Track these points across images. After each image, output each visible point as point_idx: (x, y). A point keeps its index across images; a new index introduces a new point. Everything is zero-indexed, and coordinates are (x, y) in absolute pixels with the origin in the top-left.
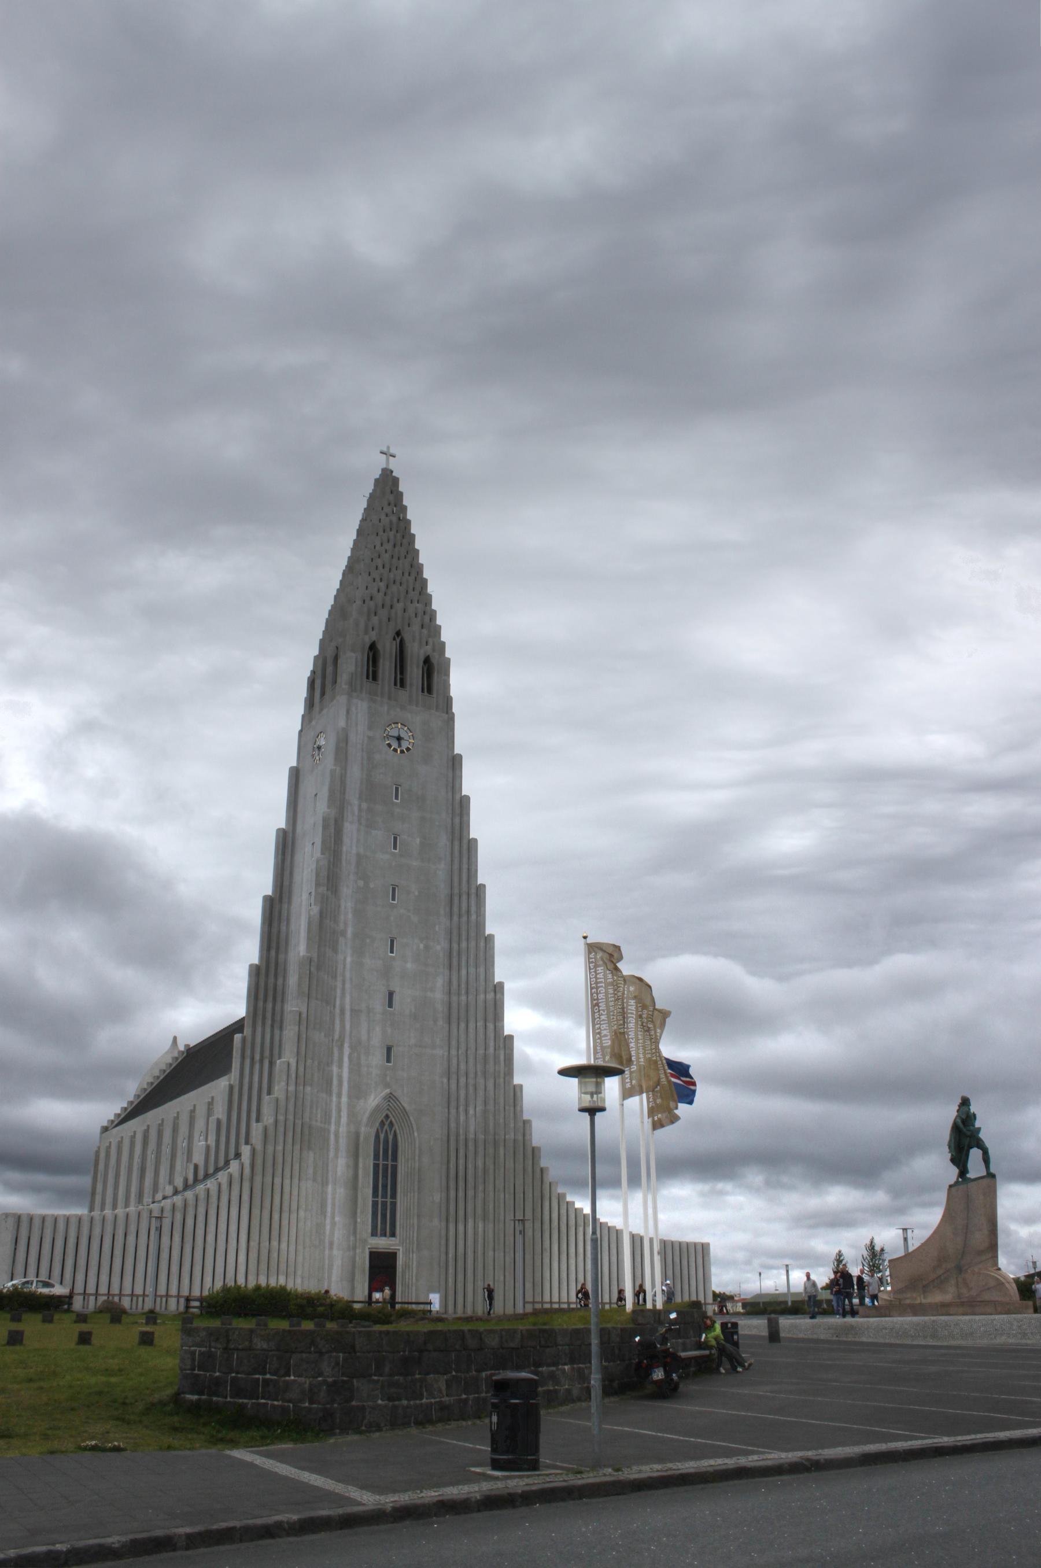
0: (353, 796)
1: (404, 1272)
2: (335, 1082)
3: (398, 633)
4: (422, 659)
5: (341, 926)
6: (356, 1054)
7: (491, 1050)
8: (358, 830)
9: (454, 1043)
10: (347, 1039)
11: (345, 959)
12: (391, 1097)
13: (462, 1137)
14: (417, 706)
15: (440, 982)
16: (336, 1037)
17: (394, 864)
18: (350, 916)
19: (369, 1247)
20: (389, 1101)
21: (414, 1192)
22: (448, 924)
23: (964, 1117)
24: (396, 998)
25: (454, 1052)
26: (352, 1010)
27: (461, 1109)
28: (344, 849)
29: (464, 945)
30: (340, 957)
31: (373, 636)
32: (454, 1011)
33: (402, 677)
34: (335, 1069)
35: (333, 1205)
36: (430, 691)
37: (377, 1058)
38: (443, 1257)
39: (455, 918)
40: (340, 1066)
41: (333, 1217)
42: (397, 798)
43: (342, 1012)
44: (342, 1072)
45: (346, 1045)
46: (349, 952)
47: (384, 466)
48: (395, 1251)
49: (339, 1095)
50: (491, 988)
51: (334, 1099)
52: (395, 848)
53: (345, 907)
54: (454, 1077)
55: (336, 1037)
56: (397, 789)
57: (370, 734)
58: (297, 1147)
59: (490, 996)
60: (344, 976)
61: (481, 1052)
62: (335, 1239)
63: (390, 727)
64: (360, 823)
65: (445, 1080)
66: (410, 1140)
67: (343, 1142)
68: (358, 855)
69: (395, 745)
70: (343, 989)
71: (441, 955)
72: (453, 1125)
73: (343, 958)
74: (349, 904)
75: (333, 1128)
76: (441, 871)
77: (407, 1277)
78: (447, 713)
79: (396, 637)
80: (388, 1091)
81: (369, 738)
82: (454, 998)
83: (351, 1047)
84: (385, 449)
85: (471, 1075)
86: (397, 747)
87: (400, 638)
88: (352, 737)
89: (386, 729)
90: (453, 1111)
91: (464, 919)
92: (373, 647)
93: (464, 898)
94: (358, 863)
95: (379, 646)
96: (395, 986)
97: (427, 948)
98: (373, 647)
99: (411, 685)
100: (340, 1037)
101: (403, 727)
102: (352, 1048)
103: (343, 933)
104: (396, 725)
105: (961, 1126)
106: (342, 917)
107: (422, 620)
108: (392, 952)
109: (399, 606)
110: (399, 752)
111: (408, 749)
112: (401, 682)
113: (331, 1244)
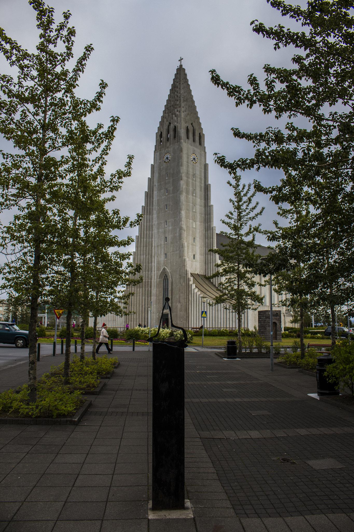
0: (156, 183)
2: (153, 268)
3: (170, 123)
4: (174, 127)
12: (164, 269)
16: (153, 255)
26: (157, 246)
30: (154, 232)
34: (153, 264)
37: (162, 258)
43: (155, 247)
49: (154, 271)
57: (160, 161)
60: (155, 237)
70: (155, 241)
75: (153, 280)
88: (155, 165)
92: (161, 133)
96: (167, 236)
102: (157, 257)
103: (155, 224)
113: (153, 312)
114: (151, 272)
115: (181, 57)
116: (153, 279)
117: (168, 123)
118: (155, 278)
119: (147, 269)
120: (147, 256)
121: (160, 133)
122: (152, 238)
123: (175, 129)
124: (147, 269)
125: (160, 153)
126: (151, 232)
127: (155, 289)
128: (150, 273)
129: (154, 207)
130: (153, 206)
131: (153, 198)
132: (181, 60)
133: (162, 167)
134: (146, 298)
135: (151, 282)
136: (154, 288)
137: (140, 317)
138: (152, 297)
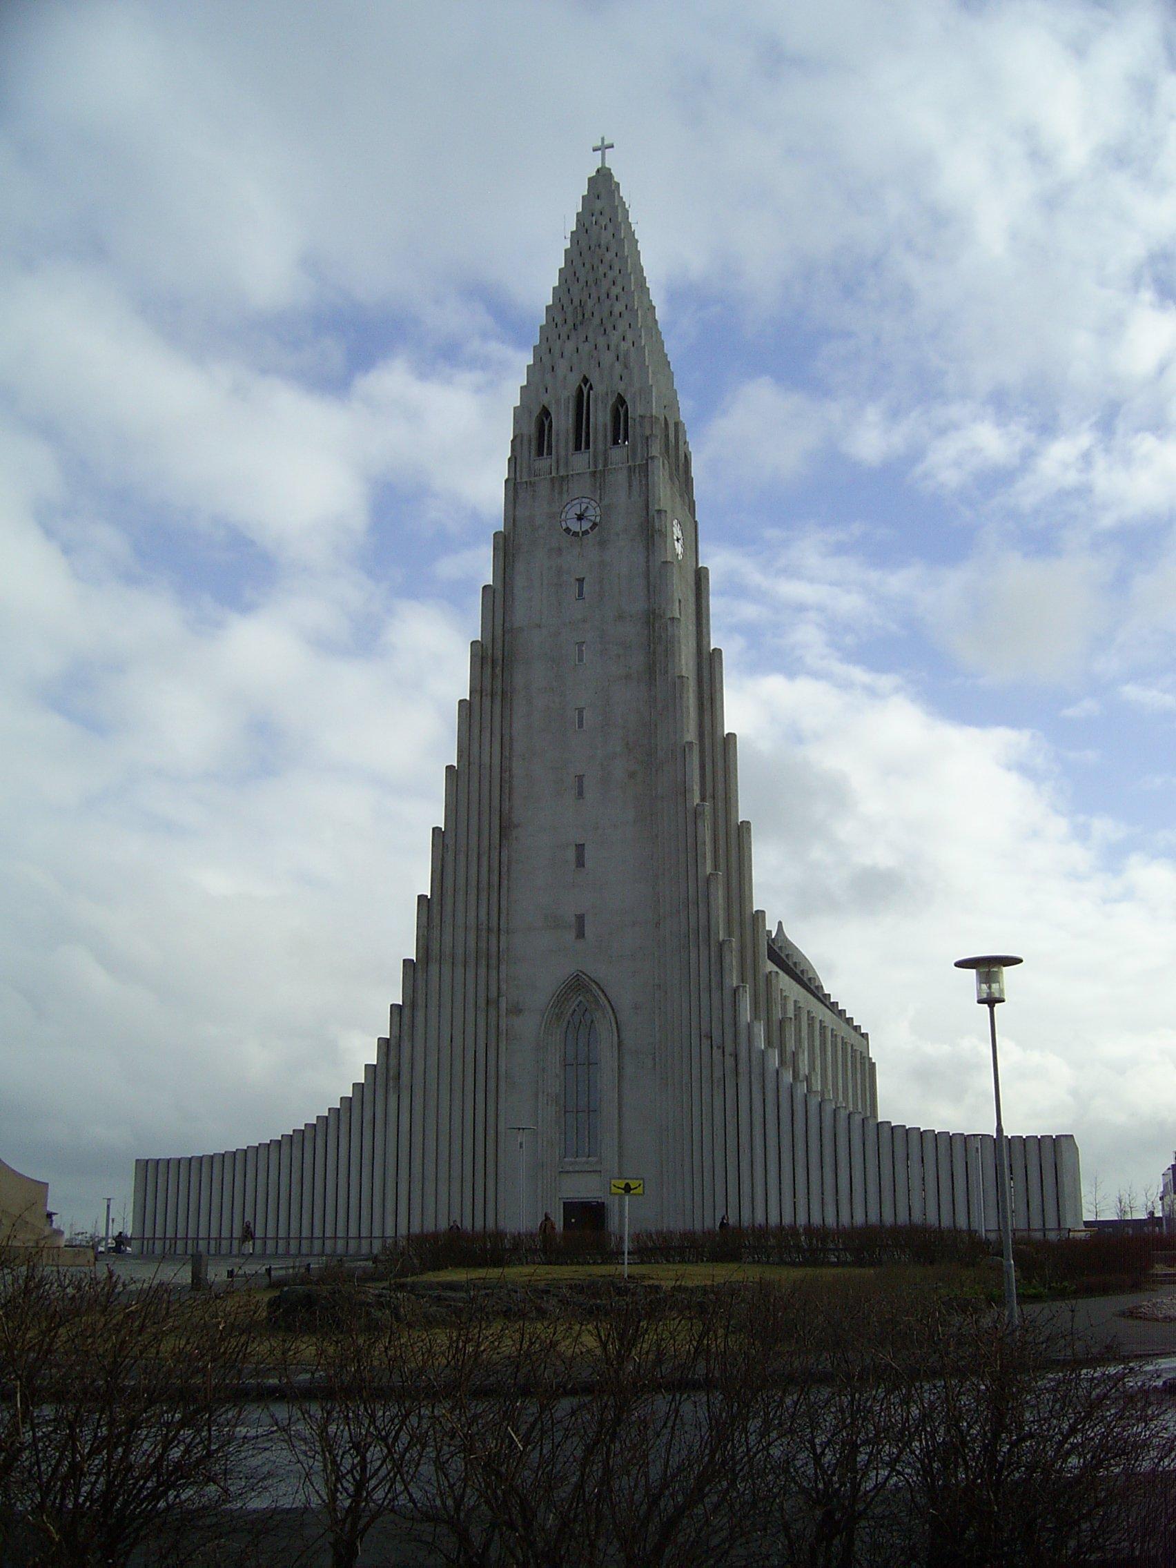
3: (585, 380)
4: (612, 400)
24: (588, 853)
31: (546, 399)
47: (600, 166)
63: (569, 506)
79: (583, 386)
84: (600, 144)
86: (578, 530)
87: (588, 386)
92: (545, 413)
95: (552, 411)
98: (545, 413)
107: (618, 346)
110: (580, 535)
111: (595, 525)
115: (603, 139)
117: (574, 381)
132: (603, 148)
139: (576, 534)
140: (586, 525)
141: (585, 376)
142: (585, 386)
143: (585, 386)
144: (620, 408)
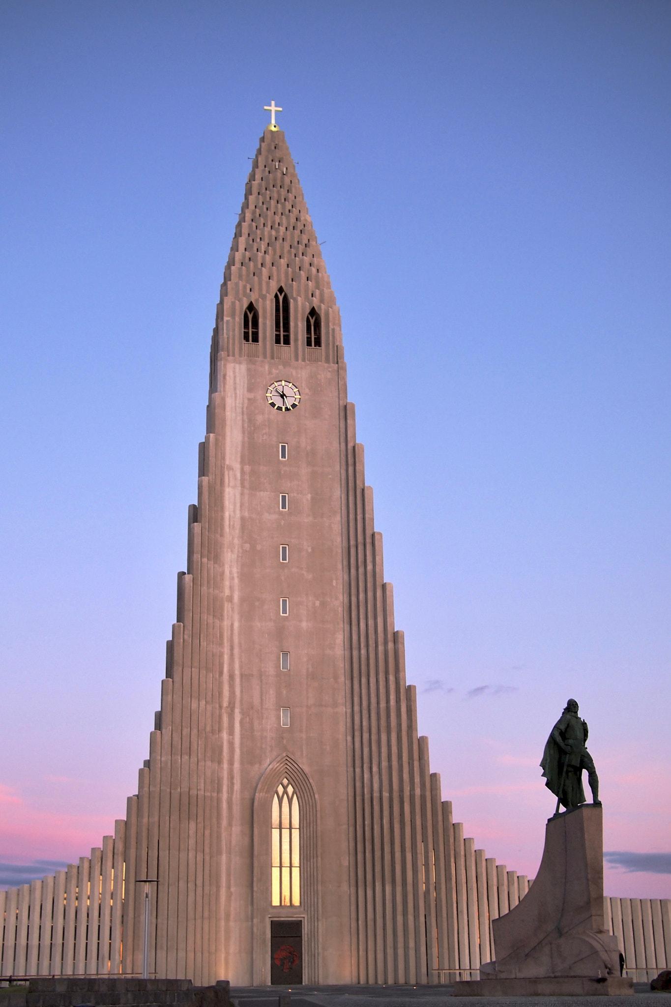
1: (309, 941)
3: (281, 290)
4: (308, 311)
5: (227, 592)
6: (248, 719)
7: (393, 702)
8: (242, 494)
9: (356, 699)
10: (237, 704)
11: (232, 625)
13: (367, 796)
14: (304, 360)
15: (340, 638)
16: (225, 704)
17: (283, 523)
18: (236, 581)
19: (269, 916)
20: (286, 764)
21: (317, 856)
22: (346, 577)
23: (563, 727)
25: (356, 708)
26: (242, 676)
27: (366, 766)
28: (227, 514)
29: (362, 596)
30: (226, 623)
32: (356, 666)
33: (285, 334)
34: (225, 735)
35: (229, 875)
36: (318, 343)
38: (354, 925)
39: (353, 571)
40: (231, 732)
41: (229, 887)
42: (283, 456)
43: (232, 677)
44: (233, 739)
45: (237, 711)
46: (236, 617)
48: (300, 919)
49: (231, 763)
50: (390, 636)
51: (225, 766)
52: (284, 507)
53: (231, 572)
54: (357, 734)
55: (225, 704)
56: (283, 448)
57: (251, 396)
58: (175, 817)
59: (391, 645)
61: (383, 705)
62: (232, 909)
64: (243, 486)
65: (349, 738)
66: (311, 804)
67: (236, 809)
68: (243, 519)
69: (279, 402)
70: (232, 655)
71: (340, 609)
72: (358, 784)
73: (230, 624)
74: (235, 570)
75: (225, 796)
76: (335, 524)
77: (313, 945)
78: (337, 363)
80: (284, 755)
81: (249, 399)
82: (355, 653)
83: (242, 712)
85: (374, 730)
89: (268, 389)
90: (358, 770)
91: (361, 570)
92: (251, 307)
93: (360, 548)
94: (243, 527)
97: (323, 604)
98: (251, 307)
99: (296, 340)
100: (230, 703)
101: (287, 383)
103: (230, 599)
104: (279, 383)
105: (559, 739)
106: (227, 583)
108: (284, 612)
109: (283, 262)
111: (294, 406)
112: (283, 337)
113: (228, 916)
114: (220, 762)
116: (225, 789)
117: (274, 289)
118: (237, 786)
119: (209, 754)
120: (209, 708)
121: (245, 305)
122: (221, 644)
123: (314, 320)
124: (209, 754)
125: (249, 370)
126: (217, 622)
127: (236, 829)
128: (216, 765)
129: (227, 539)
130: (222, 535)
131: (222, 508)
133: (259, 418)
134: (207, 858)
135: (219, 800)
136: (230, 825)
137: (199, 936)
138: (224, 858)
139: (280, 408)
140: (289, 402)
141: (281, 287)
142: (281, 295)
143: (281, 295)
144: (310, 318)
